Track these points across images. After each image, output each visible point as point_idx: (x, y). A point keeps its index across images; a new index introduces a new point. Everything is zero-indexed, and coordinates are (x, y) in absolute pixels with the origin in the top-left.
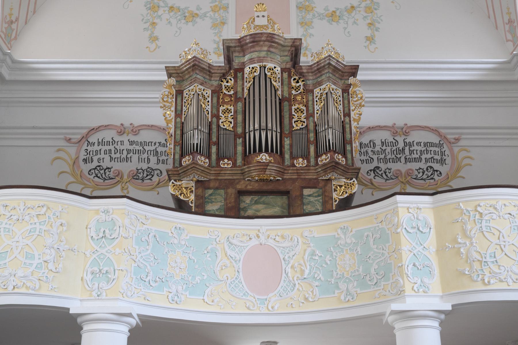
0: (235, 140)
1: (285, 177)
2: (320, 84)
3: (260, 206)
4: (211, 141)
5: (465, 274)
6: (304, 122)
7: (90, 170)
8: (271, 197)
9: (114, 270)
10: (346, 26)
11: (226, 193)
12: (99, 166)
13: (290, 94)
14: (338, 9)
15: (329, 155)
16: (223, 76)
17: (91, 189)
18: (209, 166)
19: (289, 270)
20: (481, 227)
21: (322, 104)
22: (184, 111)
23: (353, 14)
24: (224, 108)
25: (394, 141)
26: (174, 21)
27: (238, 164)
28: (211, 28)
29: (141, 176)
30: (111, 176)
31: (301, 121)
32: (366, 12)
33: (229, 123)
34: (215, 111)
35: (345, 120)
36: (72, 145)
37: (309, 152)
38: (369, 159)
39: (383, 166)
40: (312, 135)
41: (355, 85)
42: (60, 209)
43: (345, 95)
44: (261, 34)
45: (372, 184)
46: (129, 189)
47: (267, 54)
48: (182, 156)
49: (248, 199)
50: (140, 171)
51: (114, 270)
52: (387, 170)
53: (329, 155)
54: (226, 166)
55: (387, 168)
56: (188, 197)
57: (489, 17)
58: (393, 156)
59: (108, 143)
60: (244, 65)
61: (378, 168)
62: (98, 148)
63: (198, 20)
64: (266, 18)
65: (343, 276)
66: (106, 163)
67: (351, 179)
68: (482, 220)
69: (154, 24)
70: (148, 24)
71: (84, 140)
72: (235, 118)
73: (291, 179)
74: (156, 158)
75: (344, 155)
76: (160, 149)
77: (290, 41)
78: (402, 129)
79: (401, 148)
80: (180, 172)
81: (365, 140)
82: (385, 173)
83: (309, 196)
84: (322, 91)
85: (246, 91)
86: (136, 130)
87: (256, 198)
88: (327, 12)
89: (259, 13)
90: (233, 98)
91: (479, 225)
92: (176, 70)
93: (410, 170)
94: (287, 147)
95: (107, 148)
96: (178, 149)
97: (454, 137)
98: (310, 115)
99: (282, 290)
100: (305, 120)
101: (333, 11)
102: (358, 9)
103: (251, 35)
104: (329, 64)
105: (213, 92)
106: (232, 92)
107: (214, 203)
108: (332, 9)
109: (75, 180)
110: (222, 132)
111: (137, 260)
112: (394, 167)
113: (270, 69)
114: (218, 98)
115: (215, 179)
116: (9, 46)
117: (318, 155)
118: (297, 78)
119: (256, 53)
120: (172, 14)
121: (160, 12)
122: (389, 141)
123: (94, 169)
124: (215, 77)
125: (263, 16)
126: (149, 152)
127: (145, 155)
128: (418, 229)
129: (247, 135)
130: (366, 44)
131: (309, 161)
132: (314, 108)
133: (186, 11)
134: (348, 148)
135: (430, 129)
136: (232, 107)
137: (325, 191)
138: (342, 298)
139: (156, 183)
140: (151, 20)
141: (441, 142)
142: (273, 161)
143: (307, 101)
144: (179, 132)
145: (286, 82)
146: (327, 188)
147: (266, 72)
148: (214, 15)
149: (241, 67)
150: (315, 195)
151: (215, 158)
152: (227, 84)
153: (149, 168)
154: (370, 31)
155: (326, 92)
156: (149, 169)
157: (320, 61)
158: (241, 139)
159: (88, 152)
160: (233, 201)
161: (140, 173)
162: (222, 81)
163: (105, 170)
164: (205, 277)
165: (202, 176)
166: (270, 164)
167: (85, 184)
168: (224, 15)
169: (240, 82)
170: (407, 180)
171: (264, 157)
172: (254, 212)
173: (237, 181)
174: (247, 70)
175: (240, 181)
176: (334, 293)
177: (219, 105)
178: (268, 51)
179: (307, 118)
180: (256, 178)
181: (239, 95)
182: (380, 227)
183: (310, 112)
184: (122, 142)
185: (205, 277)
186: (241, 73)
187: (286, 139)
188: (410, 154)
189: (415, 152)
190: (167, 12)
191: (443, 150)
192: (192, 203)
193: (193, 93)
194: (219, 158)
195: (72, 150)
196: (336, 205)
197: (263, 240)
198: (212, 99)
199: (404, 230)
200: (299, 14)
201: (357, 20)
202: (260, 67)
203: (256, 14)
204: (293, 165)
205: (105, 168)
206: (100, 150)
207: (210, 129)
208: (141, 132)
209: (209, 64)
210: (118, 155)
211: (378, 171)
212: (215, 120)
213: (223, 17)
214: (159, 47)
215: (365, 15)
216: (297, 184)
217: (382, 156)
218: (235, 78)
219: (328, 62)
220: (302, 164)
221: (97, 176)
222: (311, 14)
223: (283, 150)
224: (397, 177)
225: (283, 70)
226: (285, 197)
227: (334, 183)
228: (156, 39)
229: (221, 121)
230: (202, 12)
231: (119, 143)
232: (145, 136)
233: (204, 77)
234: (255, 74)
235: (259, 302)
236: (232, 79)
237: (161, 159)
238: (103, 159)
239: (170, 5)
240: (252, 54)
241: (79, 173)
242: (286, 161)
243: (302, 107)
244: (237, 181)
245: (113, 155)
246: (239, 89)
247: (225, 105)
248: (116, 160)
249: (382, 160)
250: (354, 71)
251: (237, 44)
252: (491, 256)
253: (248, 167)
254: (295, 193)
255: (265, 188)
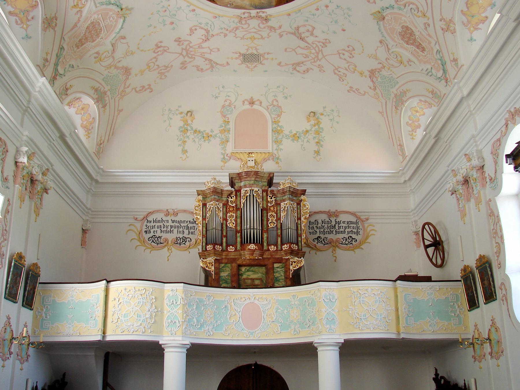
0: (236, 234)
1: (264, 257)
2: (284, 200)
3: (250, 273)
4: (223, 235)
5: (351, 324)
6: (275, 223)
7: (149, 238)
8: (256, 267)
9: (179, 322)
10: (302, 143)
11: (232, 266)
12: (154, 236)
13: (267, 206)
14: (298, 132)
15: (288, 245)
16: (230, 195)
17: (150, 250)
18: (221, 251)
19: (265, 316)
20: (360, 301)
21: (285, 213)
22: (207, 216)
23: (307, 136)
24: (230, 214)
25: (329, 221)
26: (197, 140)
27: (238, 249)
28: (219, 145)
29: (179, 242)
30: (162, 242)
31: (273, 223)
32: (315, 134)
33: (233, 224)
34: (225, 217)
35: (298, 222)
36: (137, 222)
37: (277, 242)
38: (315, 232)
39: (322, 236)
40: (279, 231)
41: (305, 201)
42: (151, 291)
43: (298, 206)
44: (251, 171)
45: (316, 247)
46: (172, 250)
47: (254, 182)
48: (207, 244)
49: (243, 269)
50: (178, 239)
51: (179, 322)
52: (325, 239)
53: (288, 245)
54: (231, 250)
55: (325, 238)
56: (211, 268)
57: (390, 138)
58: (329, 230)
59: (159, 221)
60: (241, 187)
61: (319, 237)
62: (154, 225)
63: (211, 139)
64: (254, 161)
65: (293, 322)
66: (158, 234)
67: (300, 258)
68: (360, 297)
69: (184, 142)
70: (181, 141)
71: (145, 219)
72: (236, 221)
73: (267, 258)
74: (188, 231)
75: (297, 244)
76: (190, 225)
77: (267, 174)
78: (335, 212)
79: (333, 225)
80: (206, 254)
81: (312, 220)
82: (324, 240)
83: (277, 268)
84: (285, 205)
85: (242, 205)
86: (176, 214)
87: (248, 268)
88: (291, 134)
89: (249, 158)
90: (235, 209)
91: (359, 300)
92: (202, 192)
93: (339, 238)
94: (265, 239)
95: (159, 224)
96: (204, 239)
97: (365, 217)
98: (278, 219)
99: (261, 327)
100: (275, 222)
101: (295, 134)
102: (310, 132)
103: (245, 172)
104: (289, 190)
105: (224, 205)
106: (234, 205)
107: (225, 272)
108: (294, 132)
109: (140, 244)
110: (229, 229)
111: (189, 315)
112: (329, 236)
113: (256, 192)
114: (227, 209)
115: (225, 258)
116: (99, 157)
117: (282, 244)
118: (271, 195)
119: (248, 181)
120: (195, 135)
121: (189, 133)
122: (326, 221)
123: (152, 237)
124: (225, 195)
125: (252, 161)
126: (184, 227)
127: (181, 229)
128: (330, 300)
129: (243, 231)
130: (314, 156)
131: (277, 247)
132: (280, 215)
133: (204, 133)
134: (300, 239)
135: (351, 213)
136: (234, 215)
137: (286, 265)
138: (292, 333)
139: (188, 246)
140: (183, 139)
141: (357, 221)
142: (257, 248)
143: (277, 211)
144: (204, 229)
145: (265, 199)
146: (287, 263)
147: (254, 194)
148: (222, 136)
149: (240, 189)
150: (280, 267)
151: (225, 245)
152: (231, 200)
153: (183, 237)
154: (317, 147)
155: (287, 206)
156: (183, 238)
157: (284, 188)
158: (239, 234)
159: (148, 227)
160: (235, 271)
161: (178, 240)
162: (229, 198)
163: (158, 238)
164: (223, 321)
165: (218, 257)
166: (256, 251)
167: (146, 246)
168: (228, 136)
169: (239, 198)
170: (336, 245)
171: (252, 246)
172: (247, 276)
173: (237, 259)
174: (243, 191)
175: (239, 259)
176: (288, 330)
177: (227, 213)
178: (255, 180)
179: (276, 221)
180: (248, 258)
181: (238, 207)
182: (312, 297)
183: (278, 217)
184: (168, 221)
185: (223, 321)
186: (239, 193)
187: (264, 234)
188: (339, 229)
189: (341, 227)
190: (192, 134)
191: (358, 226)
192: (213, 272)
193: (212, 207)
194: (228, 245)
195: (138, 225)
196: (292, 273)
197: (252, 300)
198: (223, 209)
199: (323, 301)
200: (274, 135)
201: (310, 139)
202: (250, 191)
203: (249, 159)
204: (268, 250)
205: (158, 237)
206: (155, 226)
207: (222, 227)
208: (178, 214)
209: (221, 189)
210: (165, 229)
211: (319, 239)
212: (225, 222)
213: (227, 137)
214: (188, 157)
215: (315, 136)
216: (271, 261)
217: (322, 230)
218: (236, 195)
219: (289, 189)
220: (274, 249)
221: (153, 242)
222: (281, 135)
223: (263, 240)
224: (331, 243)
225: (263, 191)
226: (264, 268)
227: (291, 260)
228: (186, 151)
229: (228, 222)
230: (214, 133)
231: (166, 221)
232: (181, 217)
233: (219, 197)
234: (247, 195)
235: (250, 334)
236: (234, 196)
237: (190, 231)
238: (157, 231)
239: (194, 129)
240: (246, 182)
241: (142, 240)
242: (265, 247)
243: (274, 214)
244: (237, 259)
245: (162, 229)
246: (238, 203)
247: (230, 213)
248: (164, 232)
249: (322, 232)
250: (303, 192)
251: (237, 176)
252: (363, 316)
253: (243, 252)
254: (270, 266)
255: (253, 263)
